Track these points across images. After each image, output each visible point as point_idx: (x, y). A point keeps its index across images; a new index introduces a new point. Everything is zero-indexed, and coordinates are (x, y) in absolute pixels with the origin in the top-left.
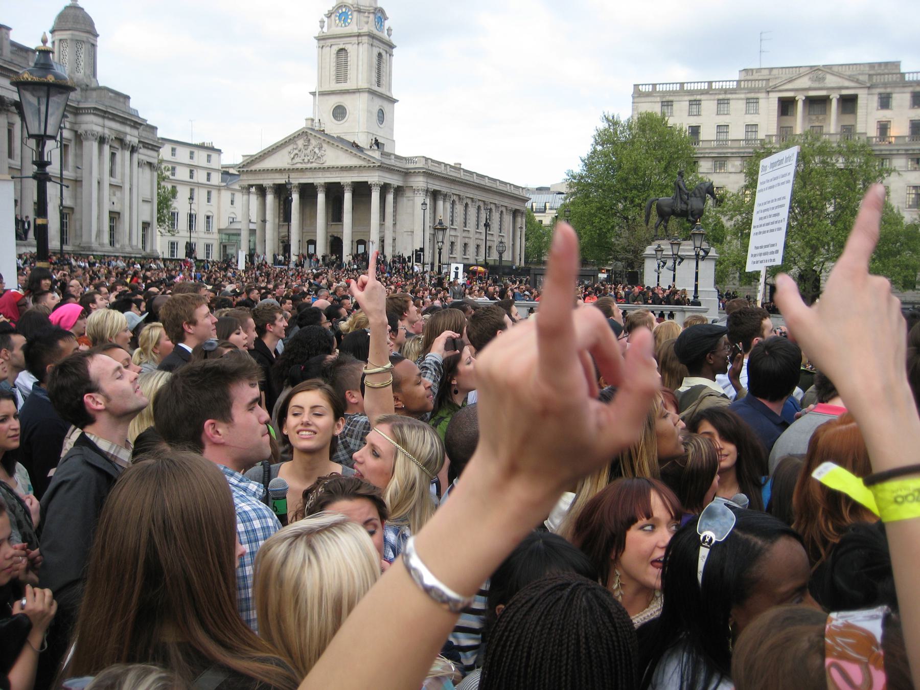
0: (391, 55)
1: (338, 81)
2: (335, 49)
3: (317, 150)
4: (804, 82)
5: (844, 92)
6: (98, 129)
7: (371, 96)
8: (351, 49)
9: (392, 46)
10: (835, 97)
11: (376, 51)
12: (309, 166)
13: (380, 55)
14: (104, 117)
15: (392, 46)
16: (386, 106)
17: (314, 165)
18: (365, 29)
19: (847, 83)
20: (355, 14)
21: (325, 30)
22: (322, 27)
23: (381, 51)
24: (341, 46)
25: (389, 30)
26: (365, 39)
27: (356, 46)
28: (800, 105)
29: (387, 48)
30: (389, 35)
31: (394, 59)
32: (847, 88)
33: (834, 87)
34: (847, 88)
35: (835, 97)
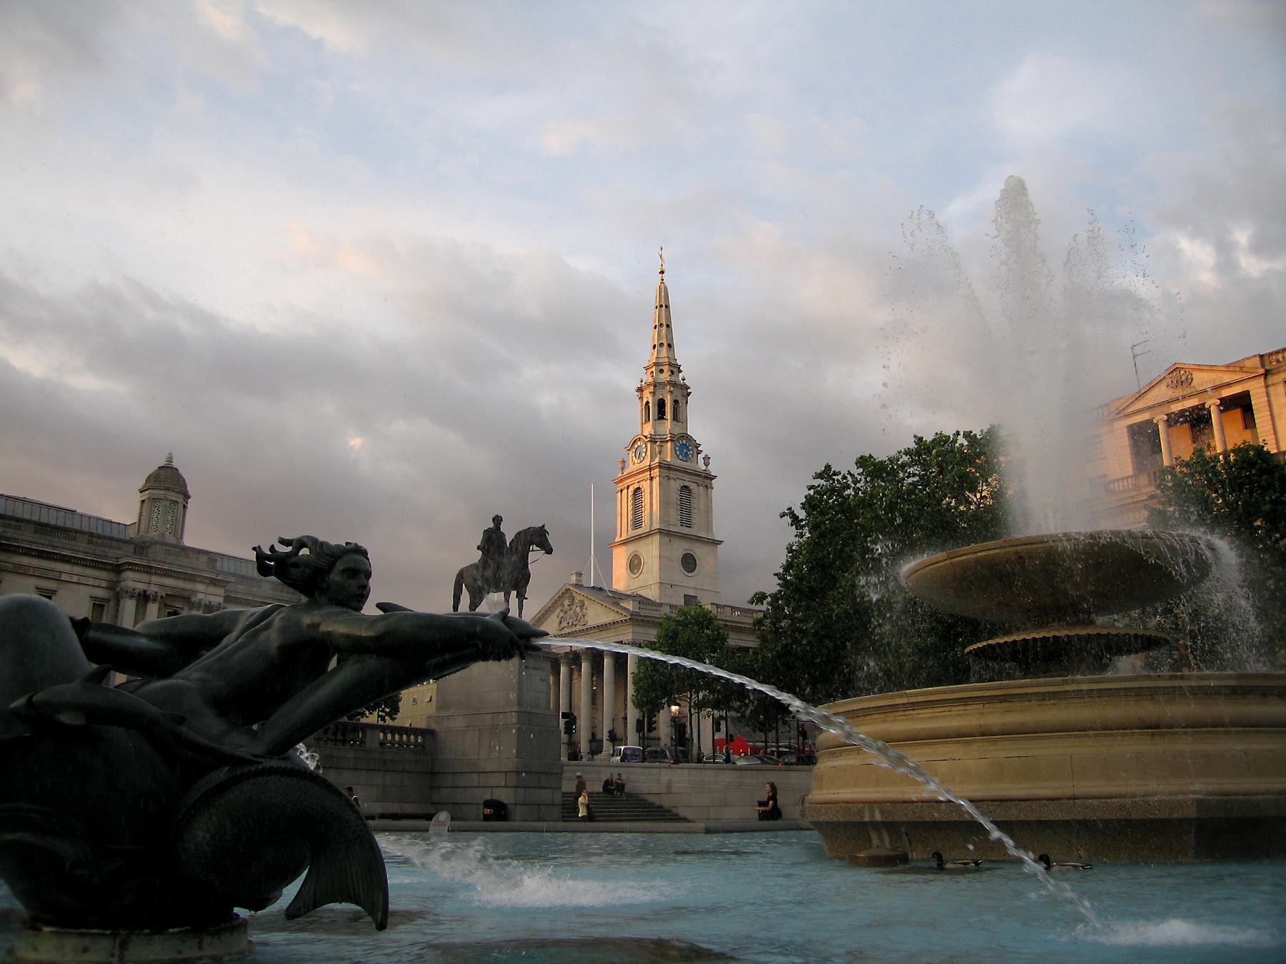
0: (708, 487)
2: (631, 489)
3: (578, 610)
4: (1163, 393)
5: (1226, 393)
6: (141, 587)
7: (667, 539)
8: (645, 486)
10: (1212, 403)
11: (675, 485)
12: (574, 629)
14: (148, 573)
17: (578, 628)
19: (1227, 378)
23: (686, 484)
24: (636, 486)
25: (707, 459)
28: (1162, 429)
29: (700, 480)
30: (707, 465)
31: (715, 493)
32: (1228, 385)
33: (1207, 388)
34: (1228, 385)
35: (1212, 403)
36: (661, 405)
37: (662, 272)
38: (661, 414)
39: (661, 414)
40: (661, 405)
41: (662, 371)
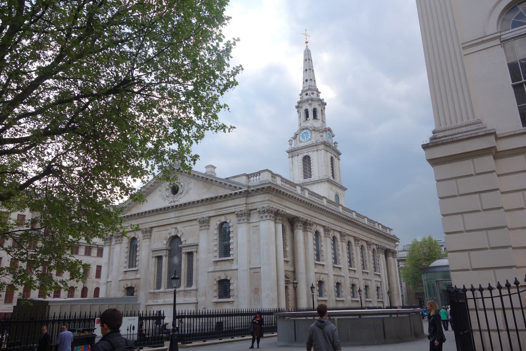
0: (339, 159)
1: (305, 177)
2: (301, 157)
9: (339, 154)
11: (329, 155)
13: (332, 158)
15: (339, 154)
16: (339, 191)
18: (321, 140)
20: (313, 132)
21: (293, 146)
22: (291, 144)
24: (306, 154)
26: (322, 147)
27: (315, 152)
30: (336, 147)
36: (315, 111)
37: (307, 42)
38: (315, 116)
39: (315, 116)
40: (315, 111)
41: (313, 93)
